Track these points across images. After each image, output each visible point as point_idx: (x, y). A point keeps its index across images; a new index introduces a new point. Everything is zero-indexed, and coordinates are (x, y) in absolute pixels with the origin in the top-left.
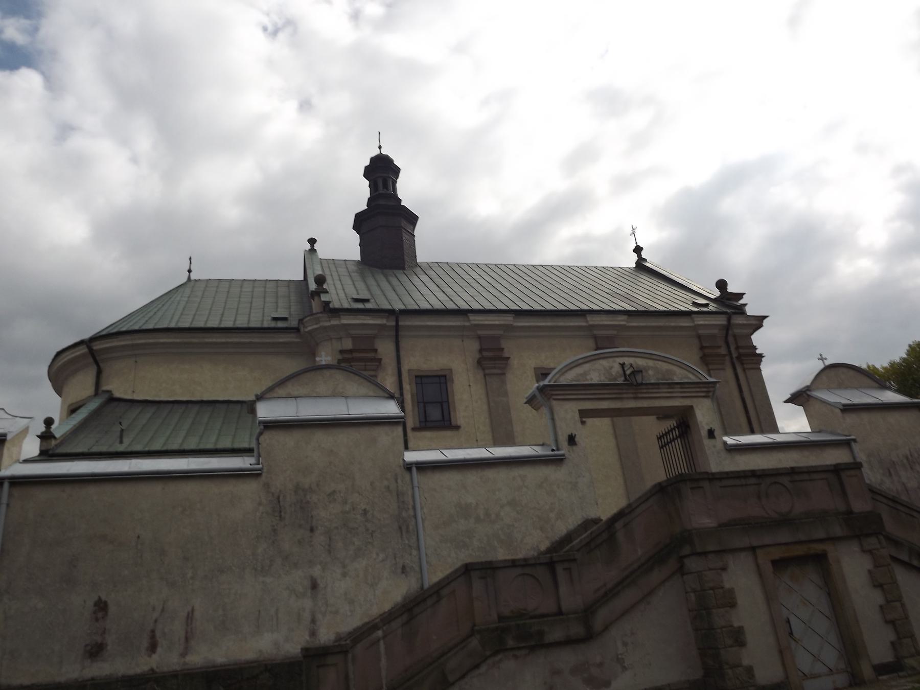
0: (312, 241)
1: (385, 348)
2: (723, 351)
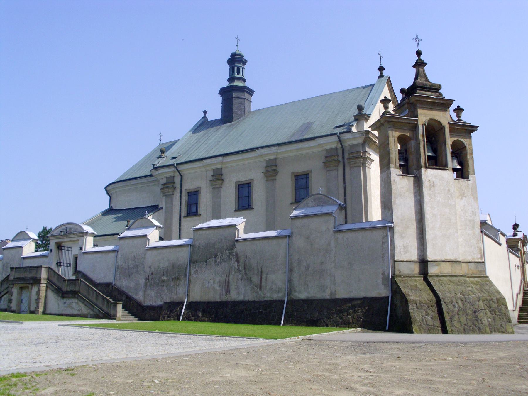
0: (205, 112)
1: (177, 180)
2: (340, 158)
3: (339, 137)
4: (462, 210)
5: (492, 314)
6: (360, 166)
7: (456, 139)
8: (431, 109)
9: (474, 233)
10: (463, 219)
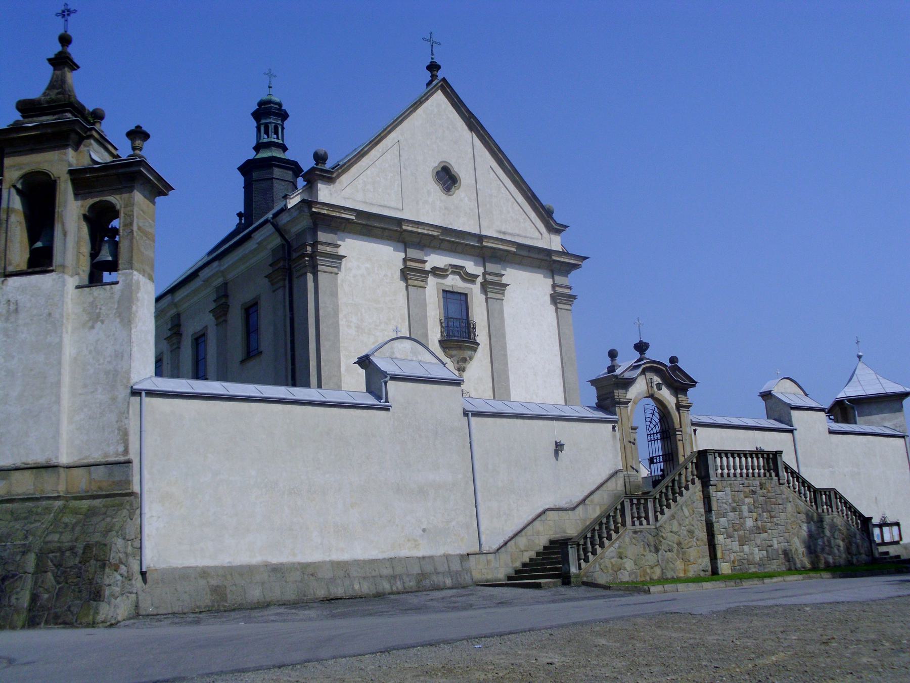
3: (273, 224)
4: (90, 352)
5: (59, 583)
6: (306, 273)
7: (97, 200)
8: (32, 151)
9: (114, 399)
10: (92, 371)
